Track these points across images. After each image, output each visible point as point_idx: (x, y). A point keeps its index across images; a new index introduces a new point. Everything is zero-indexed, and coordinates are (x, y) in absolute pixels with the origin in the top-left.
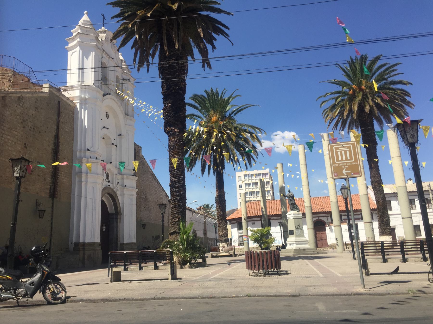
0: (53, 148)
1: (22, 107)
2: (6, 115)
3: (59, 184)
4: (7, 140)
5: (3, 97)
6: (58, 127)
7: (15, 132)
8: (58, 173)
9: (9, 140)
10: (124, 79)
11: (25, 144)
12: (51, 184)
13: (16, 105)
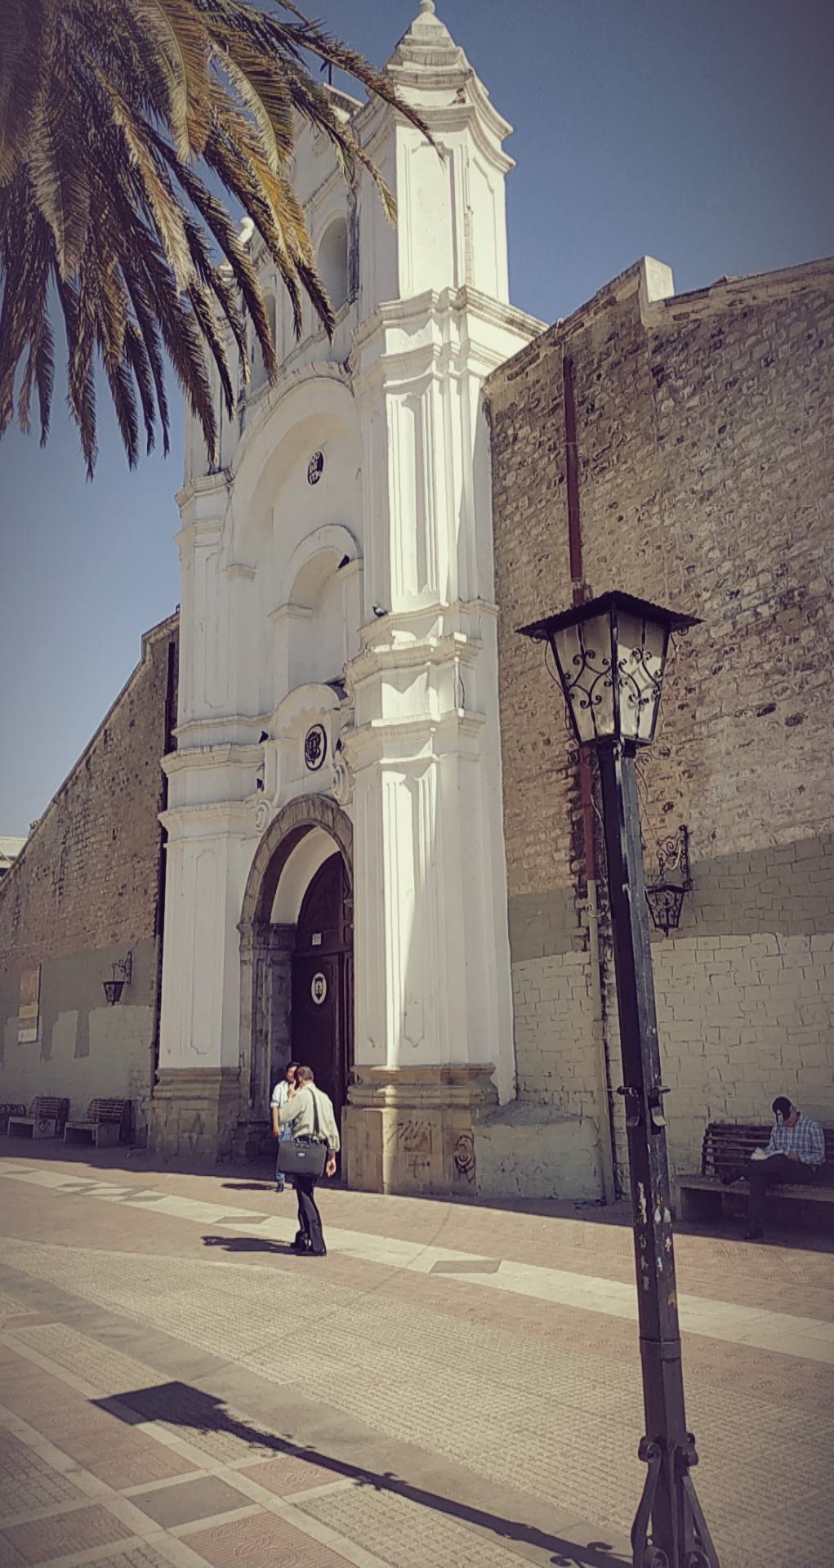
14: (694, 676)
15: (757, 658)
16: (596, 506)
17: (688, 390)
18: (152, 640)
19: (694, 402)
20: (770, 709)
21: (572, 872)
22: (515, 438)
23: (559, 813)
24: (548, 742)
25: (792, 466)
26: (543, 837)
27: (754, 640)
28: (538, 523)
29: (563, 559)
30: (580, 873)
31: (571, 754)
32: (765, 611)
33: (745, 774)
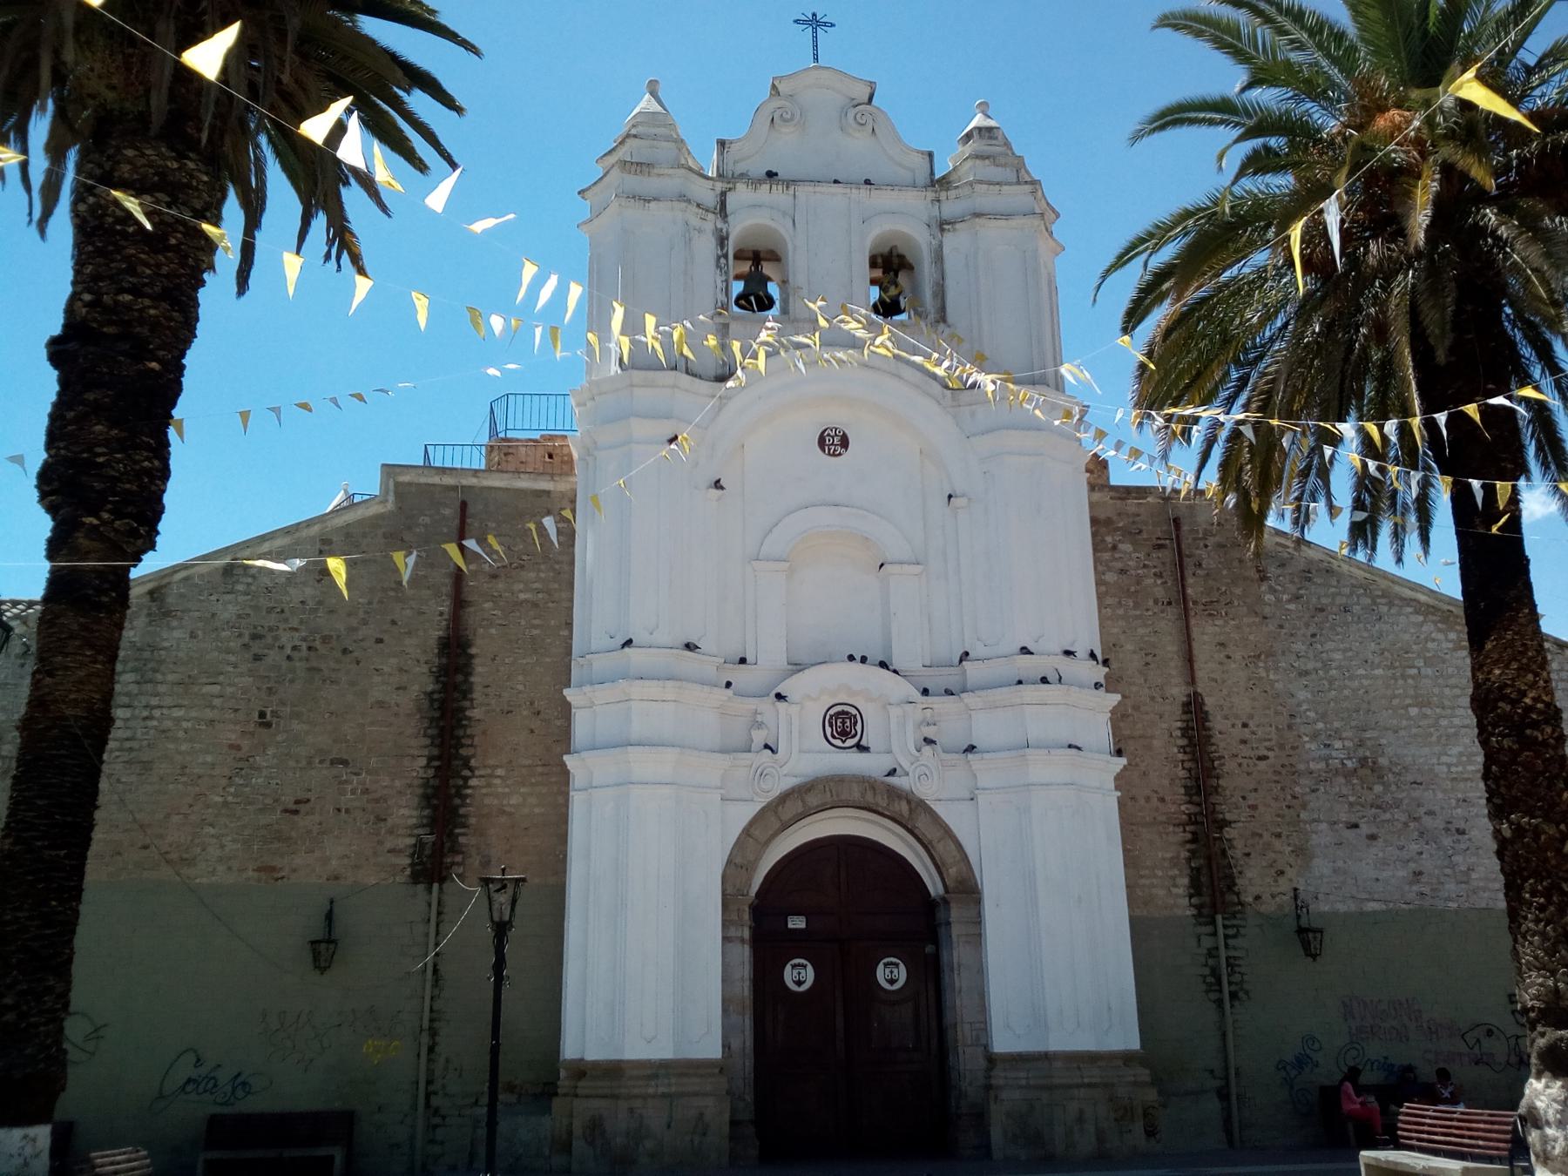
0: (430, 688)
2: (166, 644)
3: (472, 821)
4: (168, 724)
5: (151, 593)
8: (466, 779)
9: (178, 720)
11: (262, 715)
12: (420, 831)
14: (1297, 789)
15: (1345, 791)
17: (1285, 597)
18: (405, 478)
19: (1292, 607)
20: (1356, 826)
22: (1114, 548)
23: (1178, 857)
24: (1162, 800)
25: (1366, 682)
26: (1160, 873)
27: (1342, 780)
28: (1146, 626)
29: (1172, 664)
30: (1199, 907)
31: (1189, 815)
32: (1349, 764)
33: (1340, 864)
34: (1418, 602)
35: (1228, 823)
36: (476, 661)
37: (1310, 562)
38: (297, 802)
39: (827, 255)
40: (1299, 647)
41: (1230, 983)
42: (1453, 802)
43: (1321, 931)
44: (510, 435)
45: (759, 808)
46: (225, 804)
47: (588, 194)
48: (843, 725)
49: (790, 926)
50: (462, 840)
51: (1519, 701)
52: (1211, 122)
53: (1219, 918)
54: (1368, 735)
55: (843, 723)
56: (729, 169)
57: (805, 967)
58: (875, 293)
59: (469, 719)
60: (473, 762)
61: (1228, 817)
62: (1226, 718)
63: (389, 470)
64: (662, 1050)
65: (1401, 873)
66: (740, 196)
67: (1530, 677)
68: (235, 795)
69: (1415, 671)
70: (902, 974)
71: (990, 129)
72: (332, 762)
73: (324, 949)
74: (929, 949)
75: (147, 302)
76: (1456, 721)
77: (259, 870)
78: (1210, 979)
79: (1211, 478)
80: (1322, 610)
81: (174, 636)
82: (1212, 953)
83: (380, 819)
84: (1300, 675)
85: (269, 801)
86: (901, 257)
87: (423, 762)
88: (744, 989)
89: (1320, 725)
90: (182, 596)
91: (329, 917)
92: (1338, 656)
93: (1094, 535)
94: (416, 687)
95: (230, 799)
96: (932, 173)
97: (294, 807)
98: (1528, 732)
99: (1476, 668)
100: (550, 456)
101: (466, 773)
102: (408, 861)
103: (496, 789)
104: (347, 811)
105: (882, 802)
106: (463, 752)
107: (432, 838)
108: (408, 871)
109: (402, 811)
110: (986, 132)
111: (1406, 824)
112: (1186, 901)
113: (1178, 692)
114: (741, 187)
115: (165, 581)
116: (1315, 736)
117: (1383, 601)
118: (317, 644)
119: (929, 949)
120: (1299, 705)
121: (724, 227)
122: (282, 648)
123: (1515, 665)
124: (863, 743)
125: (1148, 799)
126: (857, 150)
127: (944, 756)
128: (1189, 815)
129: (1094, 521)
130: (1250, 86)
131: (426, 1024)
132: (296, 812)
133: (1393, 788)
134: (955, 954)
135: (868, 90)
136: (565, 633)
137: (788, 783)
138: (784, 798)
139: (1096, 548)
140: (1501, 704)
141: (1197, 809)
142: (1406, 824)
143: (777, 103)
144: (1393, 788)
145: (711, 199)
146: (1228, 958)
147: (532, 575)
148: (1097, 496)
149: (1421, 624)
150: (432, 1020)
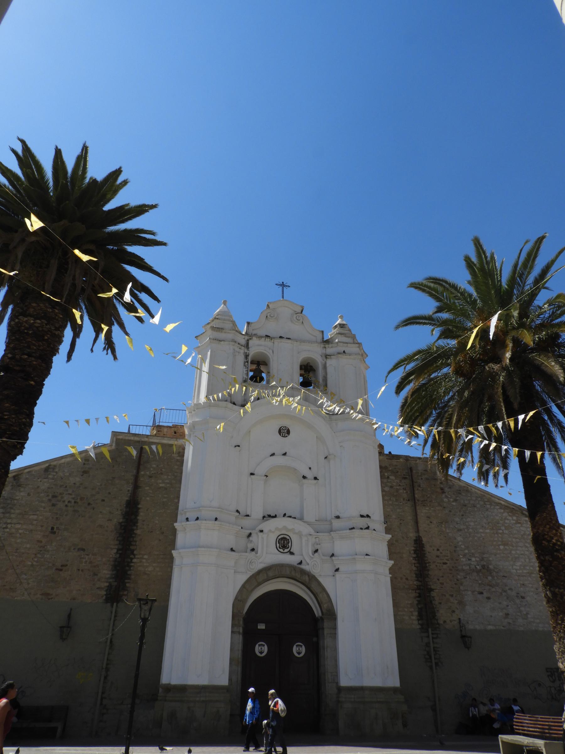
0: (121, 520)
1: (53, 479)
2: (17, 498)
3: (133, 577)
4: (13, 531)
6: (136, 487)
7: (31, 517)
8: (132, 559)
9: (18, 529)
10: (327, 356)
11: (52, 528)
12: (111, 580)
13: (39, 480)
16: (422, 514)
17: (452, 500)
18: (120, 437)
19: (454, 504)
20: (482, 593)
21: (419, 624)
22: (388, 478)
24: (407, 579)
25: (483, 535)
26: (406, 610)
27: (475, 574)
30: (421, 625)
31: (417, 586)
32: (478, 567)
34: (501, 504)
35: (432, 590)
36: (140, 510)
37: (460, 486)
38: (62, 566)
39: (285, 363)
40: (457, 519)
41: (435, 659)
42: (519, 585)
43: (470, 637)
44: (161, 424)
45: (248, 576)
46: (32, 565)
47: (199, 338)
48: (284, 543)
49: (259, 627)
50: (127, 585)
51: (551, 541)
52: (425, 324)
53: (430, 630)
54: (485, 556)
55: (284, 542)
56: (251, 332)
57: (264, 645)
58: (301, 379)
59: (136, 534)
60: (135, 552)
61: (433, 587)
62: (431, 546)
63: (115, 434)
64: (204, 681)
65: (501, 614)
66: (254, 342)
67: (554, 531)
68: (37, 562)
69: (501, 531)
70: (303, 650)
71: (344, 325)
72: (79, 550)
73: (66, 630)
74: (315, 639)
75: (33, 359)
76: (518, 552)
77: (42, 594)
78: (427, 657)
79: (428, 451)
80: (465, 506)
81: (21, 495)
82: (427, 645)
83: (95, 574)
84: (458, 530)
85: (50, 565)
86: (311, 366)
87: (115, 551)
88: (239, 654)
89: (466, 551)
90: (27, 478)
91: (69, 616)
92: (472, 524)
93: (381, 472)
94: (115, 520)
95: (35, 563)
96: (323, 338)
97: (60, 568)
98: (555, 553)
99: (533, 527)
100: (175, 433)
101: (132, 556)
102: (105, 593)
103: (144, 564)
104: (82, 570)
105: (298, 576)
106: (132, 547)
107: (115, 584)
108: (104, 598)
109: (104, 572)
110: (342, 326)
111: (501, 593)
112: (416, 622)
113: (412, 535)
114: (254, 338)
115: (20, 473)
116: (464, 555)
117: (488, 503)
118: (78, 500)
119: (315, 639)
120: (458, 543)
121: (248, 352)
122: (64, 501)
123: (548, 527)
124: (291, 551)
125: (401, 578)
126: (296, 329)
127: (323, 558)
128: (417, 586)
129: (381, 467)
130: (436, 312)
131: (104, 666)
132: (61, 570)
133: (496, 578)
134: (325, 642)
135: (301, 309)
136: (176, 501)
137: (261, 566)
138: (259, 572)
139: (382, 477)
140: (544, 542)
141: (419, 583)
142: (501, 593)
143: (268, 311)
144: (496, 578)
145: (243, 342)
146: (434, 648)
147: (166, 477)
148: (381, 457)
149: (503, 513)
150: (107, 664)
